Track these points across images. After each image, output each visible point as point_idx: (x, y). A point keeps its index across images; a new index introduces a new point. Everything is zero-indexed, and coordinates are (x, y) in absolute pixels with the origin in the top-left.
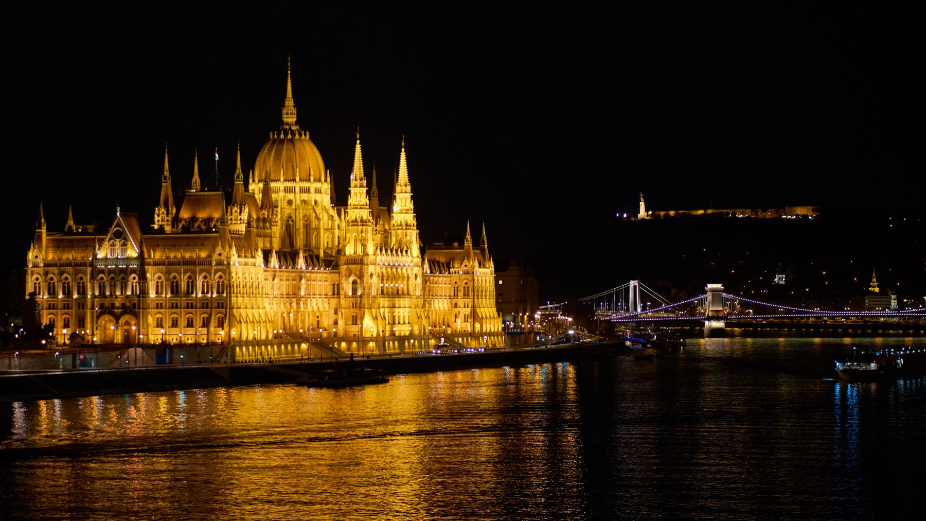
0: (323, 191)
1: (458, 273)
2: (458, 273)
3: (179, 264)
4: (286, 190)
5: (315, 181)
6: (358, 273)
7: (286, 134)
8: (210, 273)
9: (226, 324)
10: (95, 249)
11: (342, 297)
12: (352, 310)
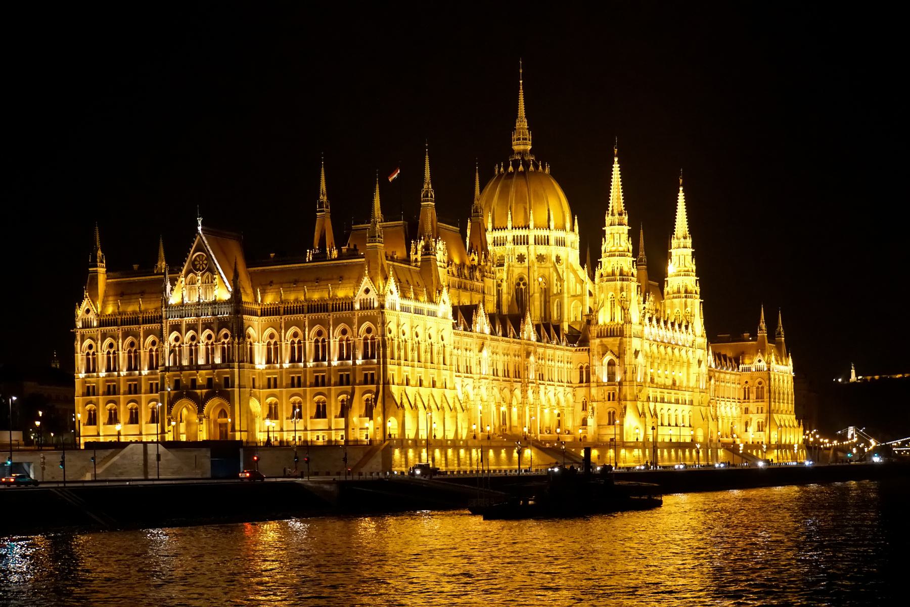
0: (568, 243)
1: (749, 370)
2: (749, 370)
3: (300, 311)
4: (516, 241)
5: (556, 228)
6: (616, 349)
7: (516, 166)
8: (351, 325)
9: (378, 409)
11: (592, 385)
12: (609, 404)
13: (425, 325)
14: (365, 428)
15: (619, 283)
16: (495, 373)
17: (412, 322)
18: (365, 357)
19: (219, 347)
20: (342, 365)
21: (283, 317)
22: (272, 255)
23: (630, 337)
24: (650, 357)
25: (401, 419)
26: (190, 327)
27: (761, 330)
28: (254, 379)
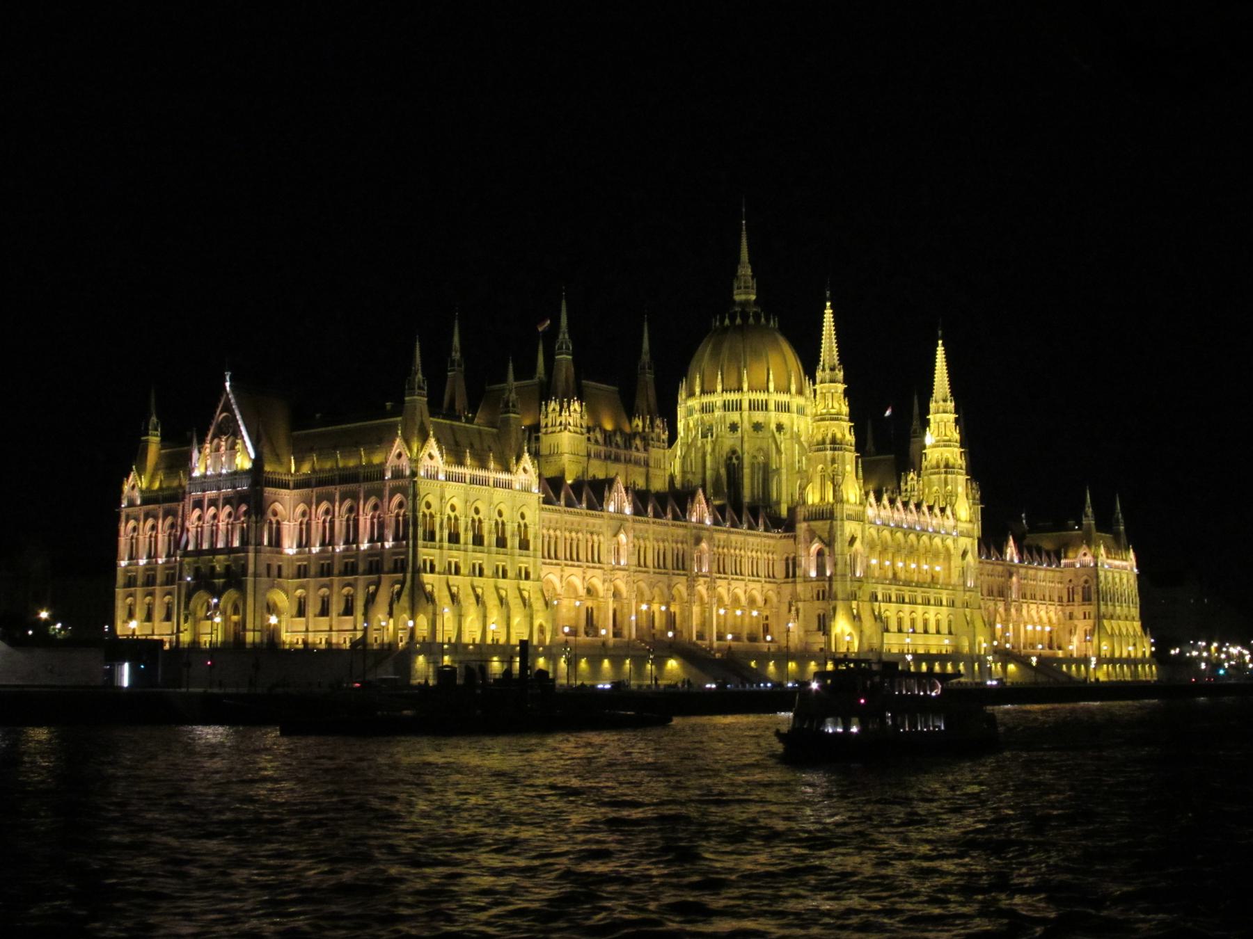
2: (1073, 565)
4: (726, 407)
5: (777, 390)
6: (825, 535)
7: (733, 319)
8: (380, 494)
10: (190, 459)
11: (798, 580)
13: (491, 498)
14: (388, 627)
15: (829, 453)
16: (641, 564)
17: (467, 494)
18: (396, 538)
19: (238, 526)
20: (371, 548)
21: (315, 490)
22: (318, 415)
23: (842, 520)
24: (872, 546)
25: (430, 616)
26: (213, 503)
27: (1086, 516)
28: (280, 568)
